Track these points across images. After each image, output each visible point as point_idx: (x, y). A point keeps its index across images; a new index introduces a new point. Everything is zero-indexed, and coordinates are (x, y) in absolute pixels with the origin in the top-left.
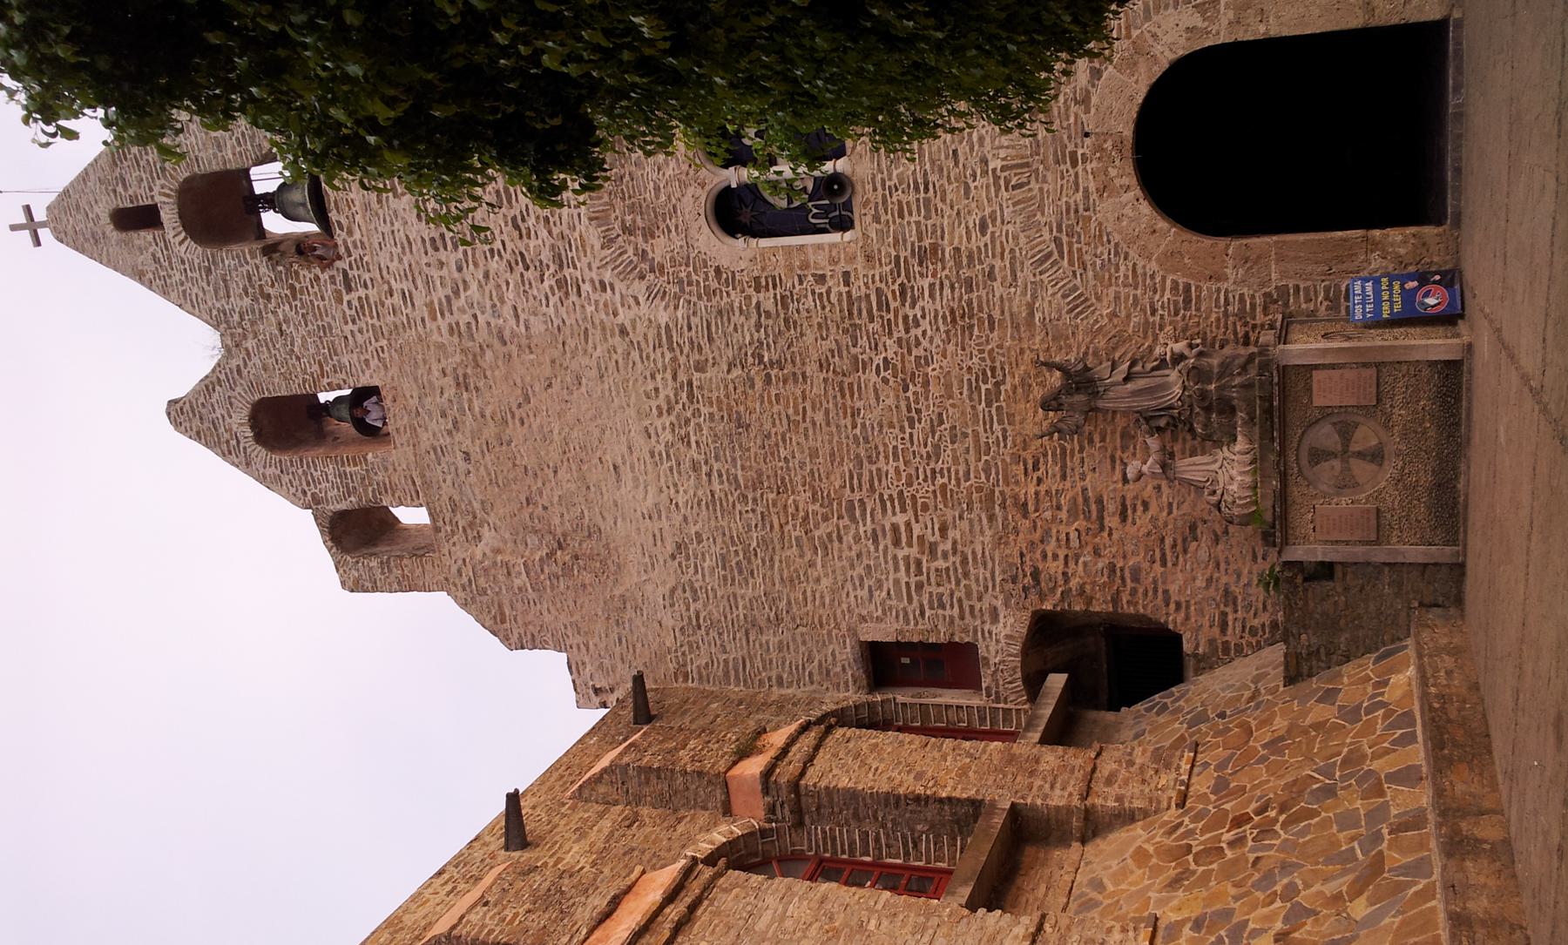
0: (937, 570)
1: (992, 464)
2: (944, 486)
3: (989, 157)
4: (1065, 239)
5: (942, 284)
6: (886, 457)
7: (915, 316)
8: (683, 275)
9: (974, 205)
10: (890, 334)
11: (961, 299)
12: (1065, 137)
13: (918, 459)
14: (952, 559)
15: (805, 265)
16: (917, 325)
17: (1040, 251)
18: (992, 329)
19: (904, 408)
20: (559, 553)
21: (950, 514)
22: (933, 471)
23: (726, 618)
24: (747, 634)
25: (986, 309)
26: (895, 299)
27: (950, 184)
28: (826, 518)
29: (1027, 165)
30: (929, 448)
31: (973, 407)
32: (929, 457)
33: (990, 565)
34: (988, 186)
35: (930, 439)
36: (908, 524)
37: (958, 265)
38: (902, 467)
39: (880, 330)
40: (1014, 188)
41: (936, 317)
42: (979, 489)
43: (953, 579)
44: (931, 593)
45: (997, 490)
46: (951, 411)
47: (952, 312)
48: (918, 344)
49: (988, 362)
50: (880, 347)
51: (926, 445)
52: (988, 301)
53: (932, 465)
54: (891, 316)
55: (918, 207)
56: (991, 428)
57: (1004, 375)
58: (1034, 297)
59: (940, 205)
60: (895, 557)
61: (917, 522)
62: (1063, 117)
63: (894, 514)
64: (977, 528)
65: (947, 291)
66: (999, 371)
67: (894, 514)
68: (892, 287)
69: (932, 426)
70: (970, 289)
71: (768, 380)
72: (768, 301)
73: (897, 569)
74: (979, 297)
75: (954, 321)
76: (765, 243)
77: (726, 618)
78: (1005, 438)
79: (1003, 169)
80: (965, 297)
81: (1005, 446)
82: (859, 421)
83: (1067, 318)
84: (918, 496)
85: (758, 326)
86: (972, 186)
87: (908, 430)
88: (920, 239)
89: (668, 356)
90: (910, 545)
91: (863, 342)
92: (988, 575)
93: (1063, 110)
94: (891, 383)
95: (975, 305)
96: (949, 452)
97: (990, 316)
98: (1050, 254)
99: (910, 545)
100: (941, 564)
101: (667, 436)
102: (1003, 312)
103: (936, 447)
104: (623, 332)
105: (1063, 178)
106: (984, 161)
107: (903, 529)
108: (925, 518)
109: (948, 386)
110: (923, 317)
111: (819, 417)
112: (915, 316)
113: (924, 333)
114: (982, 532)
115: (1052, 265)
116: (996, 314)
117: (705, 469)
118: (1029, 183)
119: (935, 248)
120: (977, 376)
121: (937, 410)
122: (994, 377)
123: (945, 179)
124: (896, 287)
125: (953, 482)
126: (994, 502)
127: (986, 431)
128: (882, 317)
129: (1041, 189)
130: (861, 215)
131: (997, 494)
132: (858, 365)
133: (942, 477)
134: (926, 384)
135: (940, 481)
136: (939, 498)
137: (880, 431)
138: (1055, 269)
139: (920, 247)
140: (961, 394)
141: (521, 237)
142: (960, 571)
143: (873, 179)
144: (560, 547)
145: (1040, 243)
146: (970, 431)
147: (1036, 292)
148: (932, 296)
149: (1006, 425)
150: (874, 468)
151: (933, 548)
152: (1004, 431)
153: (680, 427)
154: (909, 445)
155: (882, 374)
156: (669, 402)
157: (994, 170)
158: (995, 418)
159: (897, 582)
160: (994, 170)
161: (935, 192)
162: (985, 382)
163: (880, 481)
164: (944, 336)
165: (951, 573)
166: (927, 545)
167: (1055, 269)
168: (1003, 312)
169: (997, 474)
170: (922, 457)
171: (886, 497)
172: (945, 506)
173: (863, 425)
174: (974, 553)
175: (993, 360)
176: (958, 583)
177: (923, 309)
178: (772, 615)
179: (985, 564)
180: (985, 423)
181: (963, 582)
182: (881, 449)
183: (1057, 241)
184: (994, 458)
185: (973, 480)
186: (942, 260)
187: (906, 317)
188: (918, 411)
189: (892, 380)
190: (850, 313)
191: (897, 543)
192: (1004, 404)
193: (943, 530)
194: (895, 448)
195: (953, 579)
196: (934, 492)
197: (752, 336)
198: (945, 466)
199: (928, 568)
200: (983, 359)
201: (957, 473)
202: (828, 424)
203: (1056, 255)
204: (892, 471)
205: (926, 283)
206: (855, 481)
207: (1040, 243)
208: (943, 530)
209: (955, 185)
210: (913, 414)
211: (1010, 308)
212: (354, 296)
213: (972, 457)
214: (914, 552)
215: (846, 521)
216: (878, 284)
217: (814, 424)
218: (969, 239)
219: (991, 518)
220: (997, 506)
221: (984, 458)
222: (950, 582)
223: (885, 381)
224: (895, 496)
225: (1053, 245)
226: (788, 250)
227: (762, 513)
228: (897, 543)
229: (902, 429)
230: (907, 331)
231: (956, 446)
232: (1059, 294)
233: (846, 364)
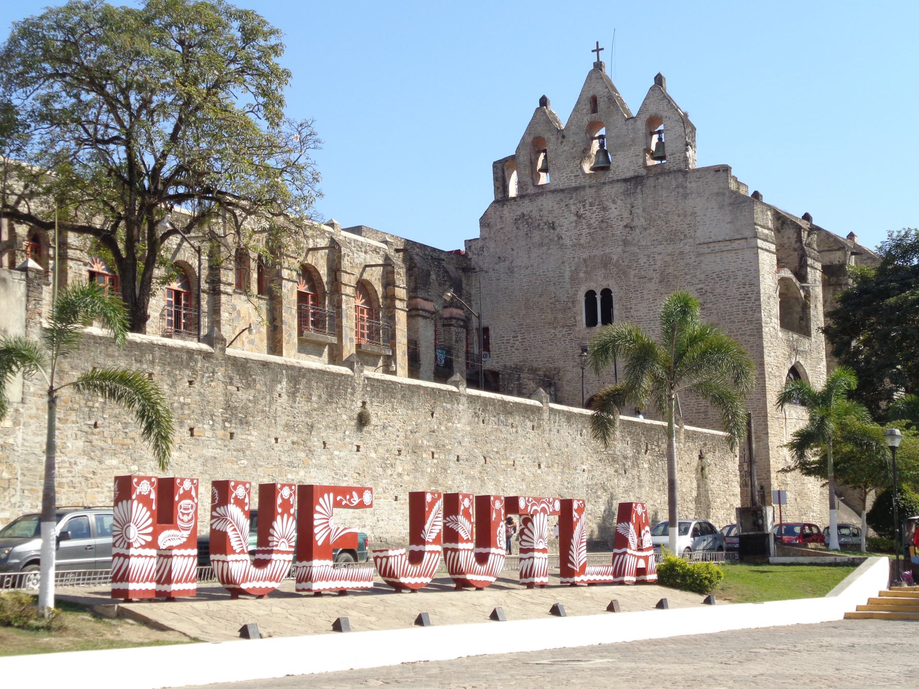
71: (552, 303)
72: (570, 304)
91: (561, 329)
100: (509, 349)
104: (563, 263)
108: (520, 344)
111: (543, 317)
132: (555, 328)
151: (513, 347)
191: (514, 337)
193: (517, 349)
212: (573, 178)
219: (520, 362)
226: (581, 311)
228: (514, 337)
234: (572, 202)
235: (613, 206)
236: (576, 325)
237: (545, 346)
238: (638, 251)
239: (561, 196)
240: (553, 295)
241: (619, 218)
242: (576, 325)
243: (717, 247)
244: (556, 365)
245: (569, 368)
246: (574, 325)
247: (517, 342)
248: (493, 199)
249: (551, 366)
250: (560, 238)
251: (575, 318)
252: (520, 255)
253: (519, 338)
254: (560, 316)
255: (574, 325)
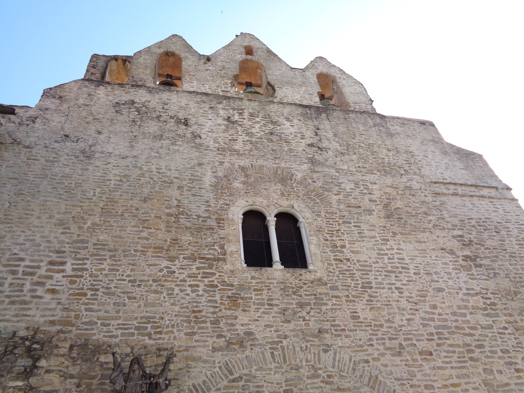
0: (23, 284)
1: (94, 327)
2: (85, 295)
3: (288, 340)
4: (241, 383)
5: (217, 307)
6: (112, 265)
7: (198, 291)
8: (226, 191)
9: (261, 329)
10: (189, 277)
11: (206, 317)
12: (301, 386)
13: (107, 282)
14: (29, 294)
15: (229, 241)
16: (193, 292)
17: (234, 367)
18: (186, 334)
19: (142, 278)
20: (92, 118)
21: (63, 297)
22: (97, 290)
23: (30, 171)
24: (15, 179)
25: (200, 331)
26: (209, 281)
27: (273, 317)
28: (80, 228)
29: (285, 361)
30: (113, 289)
31: (136, 318)
32: (108, 288)
33: (15, 319)
34: (272, 338)
35: (120, 290)
36: (63, 271)
37: (227, 317)
38: (104, 272)
39: (191, 272)
40: (272, 353)
41: (197, 302)
42: (77, 317)
43: (12, 294)
44: (6, 279)
45: (74, 329)
46: (136, 305)
47: (200, 311)
48: (181, 291)
49: (165, 330)
50: (181, 271)
51: (115, 287)
52: (205, 333)
53: (102, 290)
54: (199, 278)
55: (260, 299)
56: (120, 328)
57: (155, 340)
58: (205, 362)
59: (261, 311)
60: (41, 261)
61: (64, 277)
62: (313, 386)
63: (72, 264)
64: (47, 313)
65: (212, 310)
66: (159, 336)
67: (72, 264)
68: (216, 281)
69: (128, 293)
70: (213, 323)
71: (168, 215)
72: (212, 223)
73: (32, 261)
74: (207, 328)
75: (194, 312)
76: (240, 226)
77: (30, 171)
78: (110, 337)
79: (283, 348)
80: (208, 320)
81: (105, 336)
82: (138, 254)
83: (190, 382)
84: (82, 279)
85: (199, 216)
86: (272, 329)
87: (128, 279)
88: (242, 298)
89: (187, 178)
90: (47, 271)
91: (186, 262)
92: (7, 317)
93: (317, 385)
94: (159, 273)
95: (203, 325)
96: (108, 300)
97: (194, 333)
98: (231, 373)
99: (48, 270)
101: (145, 168)
102: (197, 341)
103: (114, 294)
105: (277, 384)
106: (286, 337)
107: (61, 268)
109: (153, 305)
110: (198, 295)
111: (145, 234)
112: (198, 291)
113: (188, 295)
114: (42, 316)
115: (226, 375)
116: (196, 337)
117: (125, 180)
118: (275, 362)
119: (237, 306)
120: (156, 323)
121: (138, 296)
122: (156, 333)
123: (275, 315)
124: (216, 283)
125: (87, 301)
126: (64, 325)
127: (119, 324)
128: (199, 274)
129: (271, 369)
130: (253, 272)
131: (70, 328)
132: (172, 259)
133: (92, 295)
134: (156, 292)
135: (89, 293)
136: (77, 291)
137: (130, 264)
138: (222, 376)
139: (238, 298)
140: (147, 312)
141: (243, 141)
142: (17, 299)
143: (274, 279)
144: (94, 119)
145: (239, 367)
146: (120, 314)
147: (208, 363)
148: (210, 301)
149: (120, 338)
150: (107, 257)
151: (42, 284)
152: (116, 337)
153: (149, 175)
154: (118, 278)
155: (165, 270)
156: (162, 173)
157: (281, 342)
158: (127, 331)
159: (22, 260)
160: (281, 342)
161: (268, 309)
162: (152, 327)
163: (97, 259)
164: (185, 305)
165: (18, 293)
166: (44, 280)
167: (222, 376)
168: (197, 341)
169: (86, 329)
170: (109, 284)
171: (86, 261)
172: (70, 295)
173: (135, 256)
174: (29, 309)
175: (166, 333)
176: (8, 297)
177: (202, 296)
178: (24, 192)
179: (16, 316)
180: (124, 324)
181: (7, 300)
182: (118, 263)
183: (241, 378)
184: (97, 328)
185: (85, 313)
186: (230, 309)
187: (198, 286)
188: (139, 286)
189: (161, 274)
190: (203, 258)
192: (135, 338)
193: (53, 291)
194: (118, 270)
195: (12, 294)
196: (82, 289)
197: (194, 212)
198: (99, 297)
199: (26, 279)
200: (168, 327)
201: (92, 304)
202: (139, 238)
203: (231, 377)
204: (103, 266)
205: (218, 298)
206: (100, 247)
207: (239, 367)
208: (53, 291)
209: (272, 320)
210: (138, 283)
211: (199, 346)
213: (101, 314)
214: (42, 272)
215: (75, 237)
216: (218, 274)
217: (141, 231)
218: (242, 325)
219: (52, 323)
220: (61, 327)
221: (99, 322)
222: (11, 291)
223: (161, 270)
224: (85, 266)
225: (236, 375)
227: (92, 199)
229: (129, 276)
230: (190, 286)
231: (112, 305)
232: (207, 380)
233: (173, 253)
234: (220, 106)
235: (288, 124)
236: (224, 260)
237: (137, 292)
238: (337, 174)
239: (204, 98)
240: (175, 203)
241: (299, 135)
242: (224, 260)
243: (460, 190)
244: (165, 340)
245: (202, 352)
246: (219, 260)
247: (59, 276)
248: (83, 78)
249: (148, 341)
250: (196, 136)
251: (222, 247)
252: (112, 140)
253: (68, 268)
254: (186, 238)
255: (219, 260)
